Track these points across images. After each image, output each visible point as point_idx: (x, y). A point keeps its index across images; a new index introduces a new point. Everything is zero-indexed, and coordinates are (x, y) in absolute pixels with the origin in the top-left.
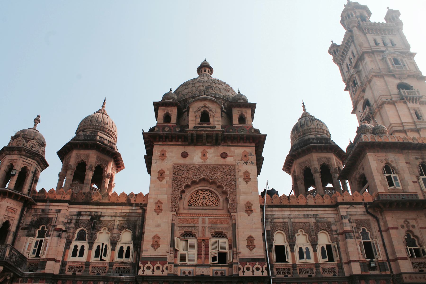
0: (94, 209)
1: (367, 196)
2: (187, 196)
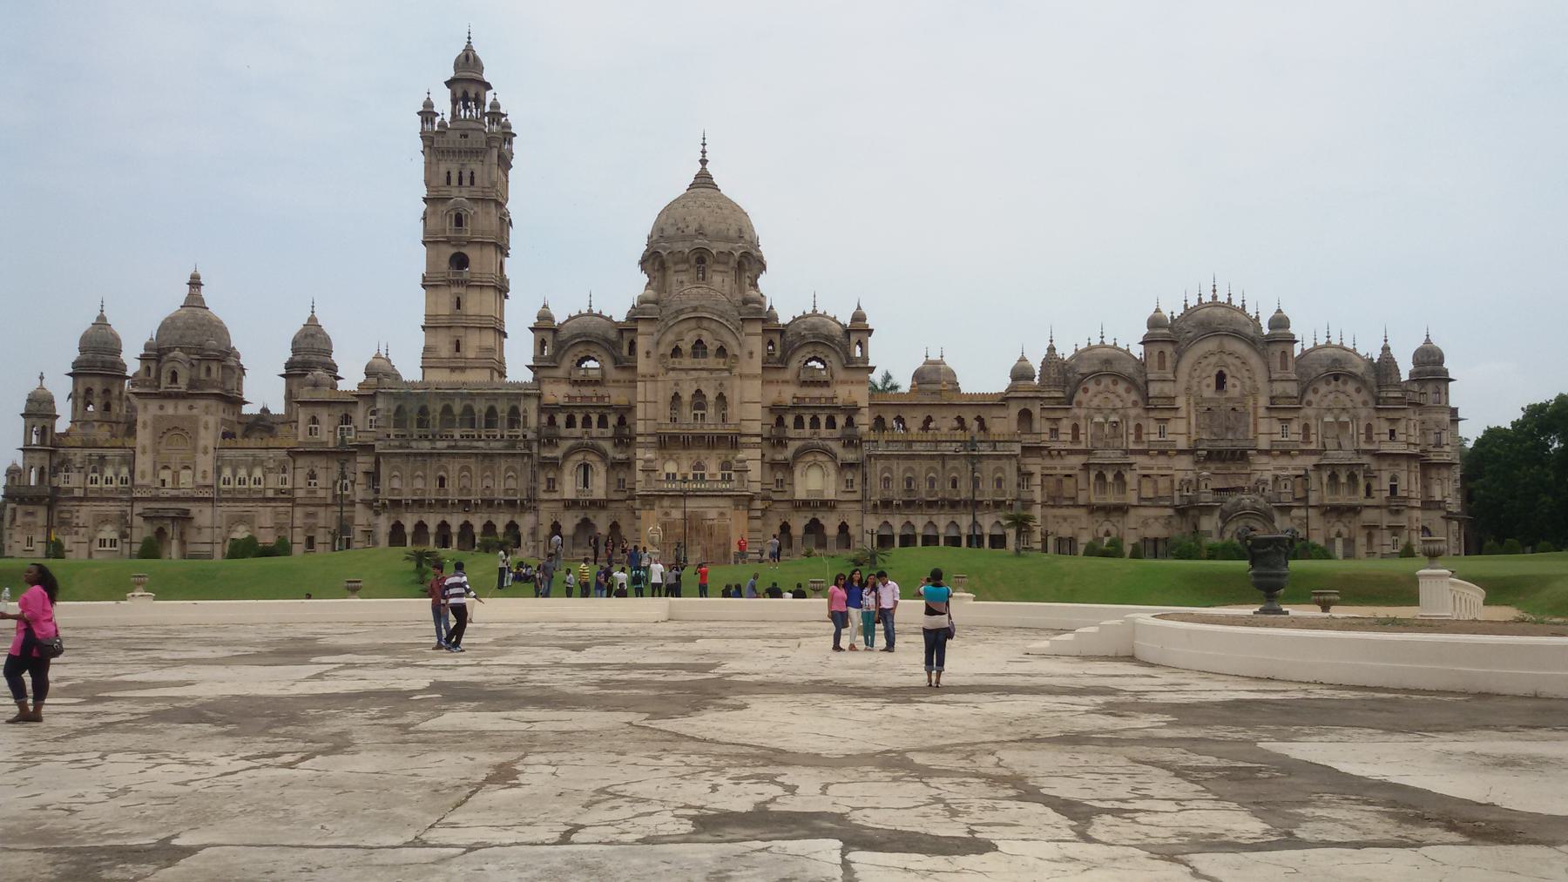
0: (100, 451)
1: (291, 443)
2: (164, 440)
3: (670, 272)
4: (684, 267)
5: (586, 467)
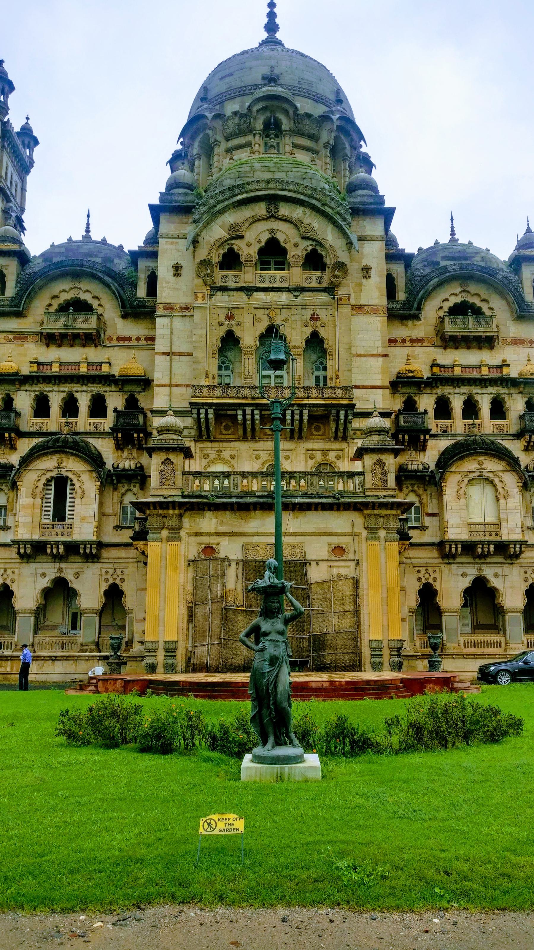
3: (219, 150)
4: (249, 138)
5: (61, 485)
